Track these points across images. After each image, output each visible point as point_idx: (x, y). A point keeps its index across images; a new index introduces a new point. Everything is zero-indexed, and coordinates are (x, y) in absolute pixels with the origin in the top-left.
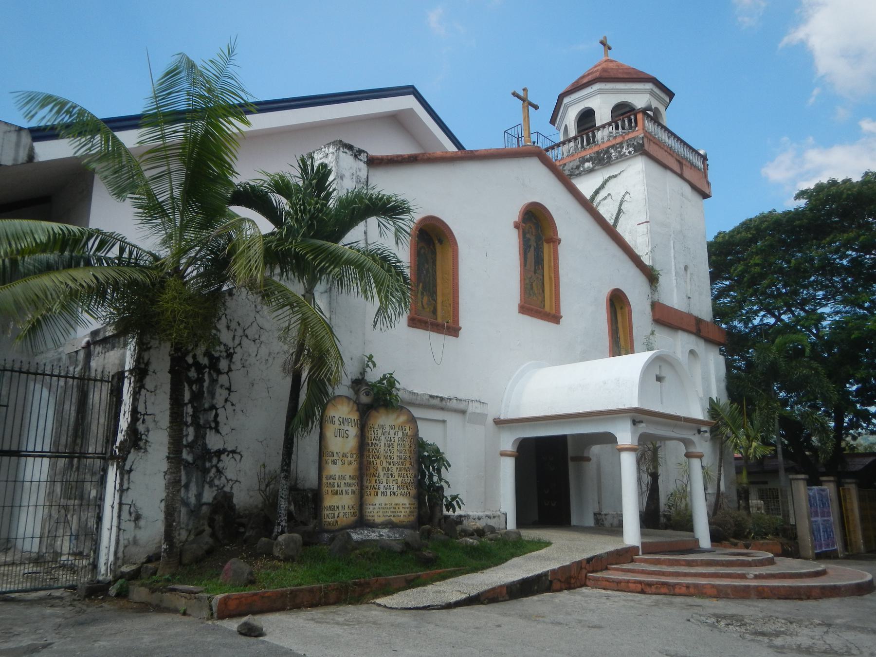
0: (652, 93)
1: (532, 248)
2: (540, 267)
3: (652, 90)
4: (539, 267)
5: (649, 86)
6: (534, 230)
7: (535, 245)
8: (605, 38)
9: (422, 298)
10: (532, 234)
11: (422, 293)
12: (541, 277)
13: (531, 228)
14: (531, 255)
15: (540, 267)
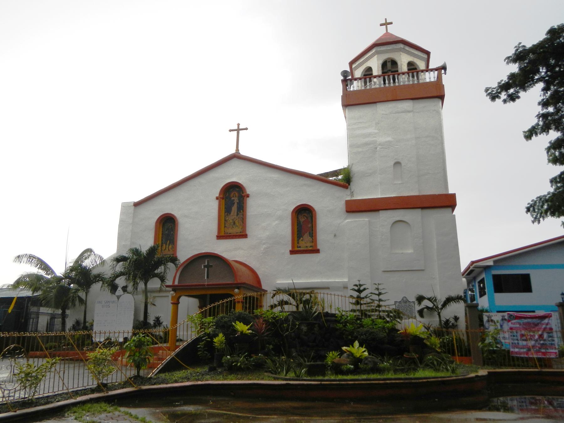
0: (377, 53)
1: (236, 205)
2: (242, 211)
3: (375, 51)
4: (240, 212)
5: (374, 51)
6: (237, 194)
7: (238, 201)
8: (386, 19)
9: (169, 247)
10: (236, 197)
11: (169, 244)
12: (242, 216)
13: (235, 194)
14: (234, 208)
15: (242, 211)
